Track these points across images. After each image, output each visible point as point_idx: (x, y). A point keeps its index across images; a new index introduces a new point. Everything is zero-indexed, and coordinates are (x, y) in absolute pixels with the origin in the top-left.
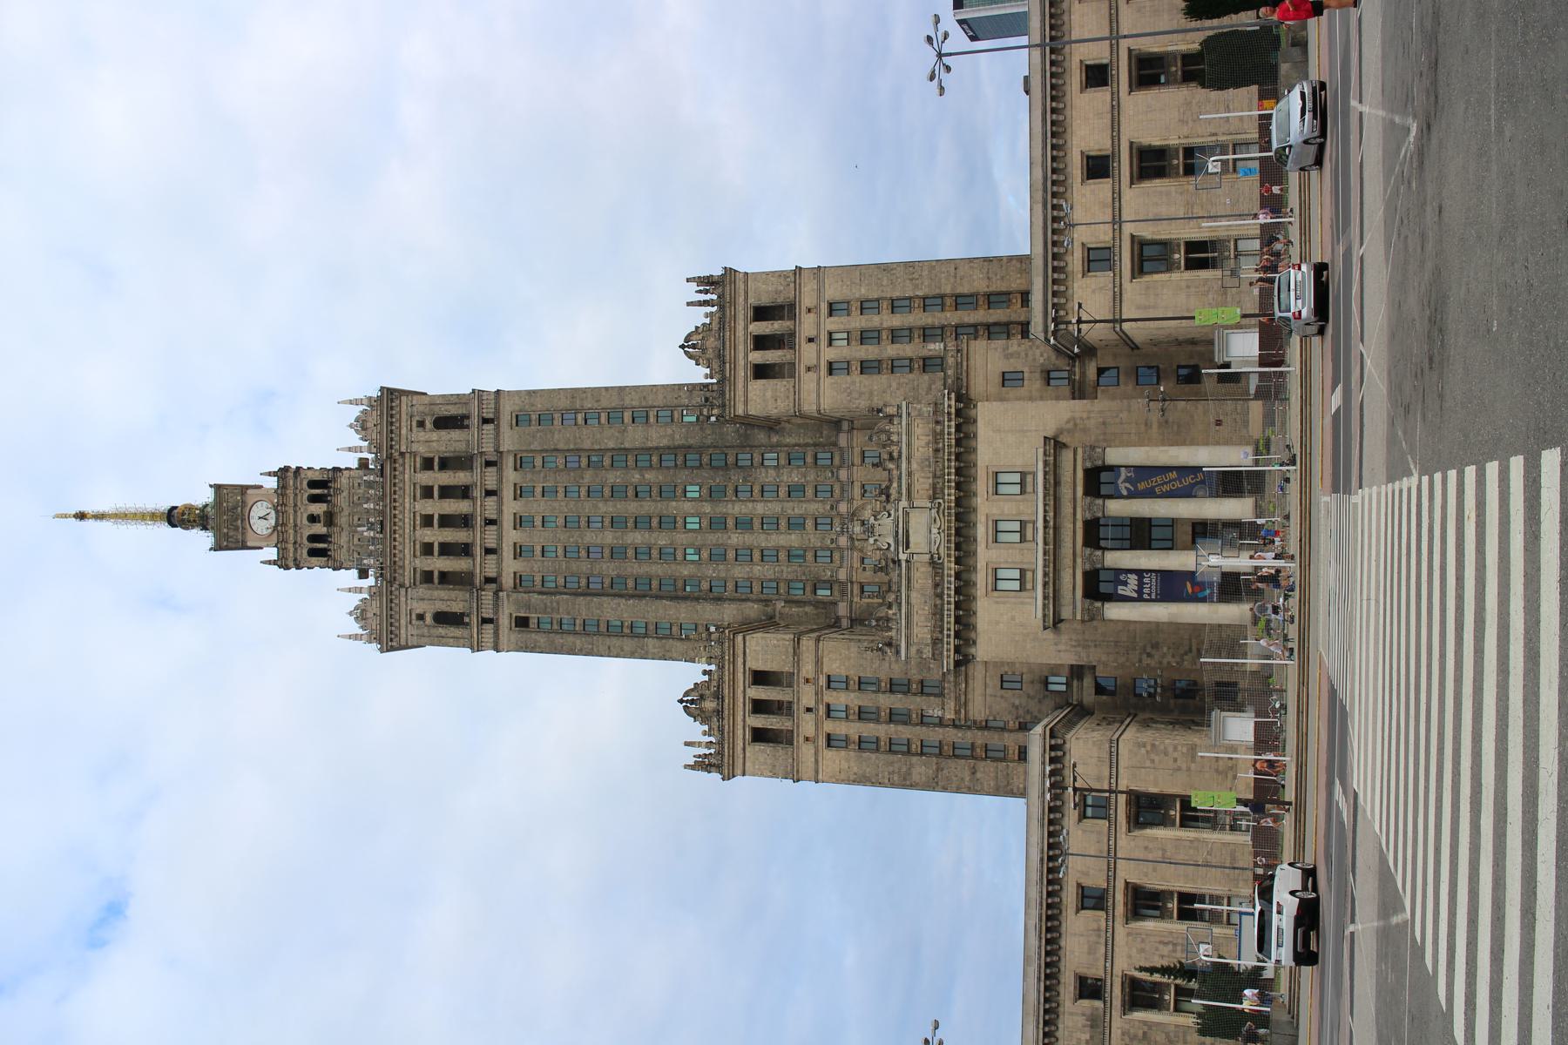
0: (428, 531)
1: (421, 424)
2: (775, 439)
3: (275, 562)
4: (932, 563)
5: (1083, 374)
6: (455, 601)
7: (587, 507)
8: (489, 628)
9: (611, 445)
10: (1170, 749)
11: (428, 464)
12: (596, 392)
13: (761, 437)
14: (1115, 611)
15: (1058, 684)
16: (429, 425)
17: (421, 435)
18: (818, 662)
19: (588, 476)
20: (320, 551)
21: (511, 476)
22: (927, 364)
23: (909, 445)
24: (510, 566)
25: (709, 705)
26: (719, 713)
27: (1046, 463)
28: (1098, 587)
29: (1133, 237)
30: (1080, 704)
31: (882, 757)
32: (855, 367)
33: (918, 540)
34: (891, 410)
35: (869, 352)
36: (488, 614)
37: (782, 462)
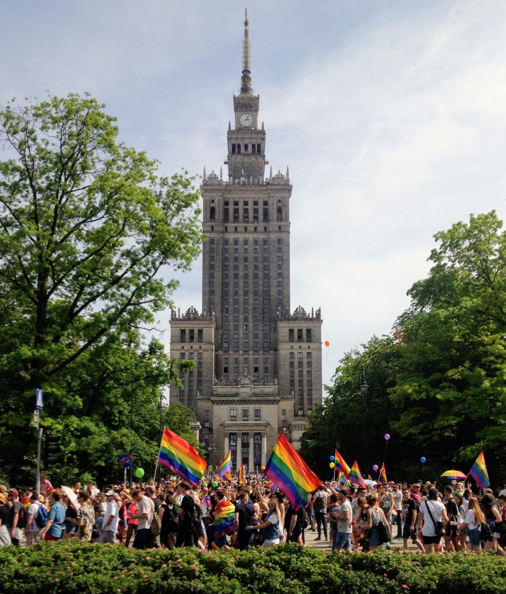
0: (242, 203)
2: (272, 330)
3: (230, 128)
4: (238, 394)
6: (219, 215)
7: (251, 265)
8: (210, 229)
9: (271, 274)
11: (266, 203)
12: (288, 269)
13: (273, 326)
16: (280, 204)
17: (275, 202)
18: (206, 350)
19: (260, 265)
21: (261, 236)
22: (292, 382)
25: (192, 316)
26: (189, 319)
32: (291, 360)
33: (243, 390)
35: (296, 364)
36: (215, 229)
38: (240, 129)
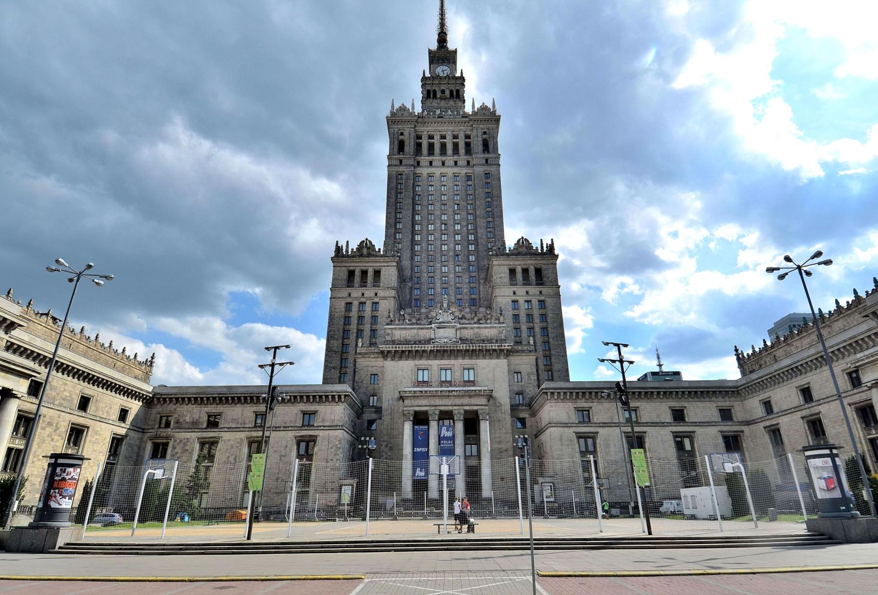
1: (485, 133)
2: (482, 281)
4: (431, 339)
5: (522, 410)
6: (409, 148)
8: (398, 163)
9: (478, 213)
10: (338, 457)
11: (467, 137)
13: (483, 275)
14: (408, 428)
15: (373, 401)
17: (480, 134)
18: (385, 298)
20: (429, 95)
21: (464, 171)
23: (486, 328)
24: (424, 171)
26: (362, 255)
27: (480, 391)
28: (420, 419)
29: (597, 433)
30: (363, 413)
31: (342, 327)
32: (516, 312)
33: (441, 333)
34: (502, 319)
37: (472, 285)
38: (434, 77)
